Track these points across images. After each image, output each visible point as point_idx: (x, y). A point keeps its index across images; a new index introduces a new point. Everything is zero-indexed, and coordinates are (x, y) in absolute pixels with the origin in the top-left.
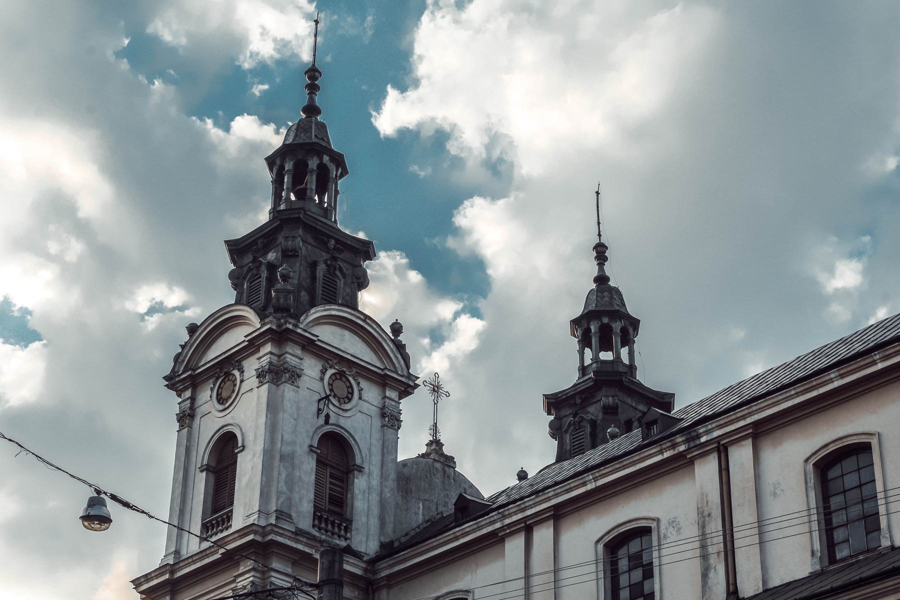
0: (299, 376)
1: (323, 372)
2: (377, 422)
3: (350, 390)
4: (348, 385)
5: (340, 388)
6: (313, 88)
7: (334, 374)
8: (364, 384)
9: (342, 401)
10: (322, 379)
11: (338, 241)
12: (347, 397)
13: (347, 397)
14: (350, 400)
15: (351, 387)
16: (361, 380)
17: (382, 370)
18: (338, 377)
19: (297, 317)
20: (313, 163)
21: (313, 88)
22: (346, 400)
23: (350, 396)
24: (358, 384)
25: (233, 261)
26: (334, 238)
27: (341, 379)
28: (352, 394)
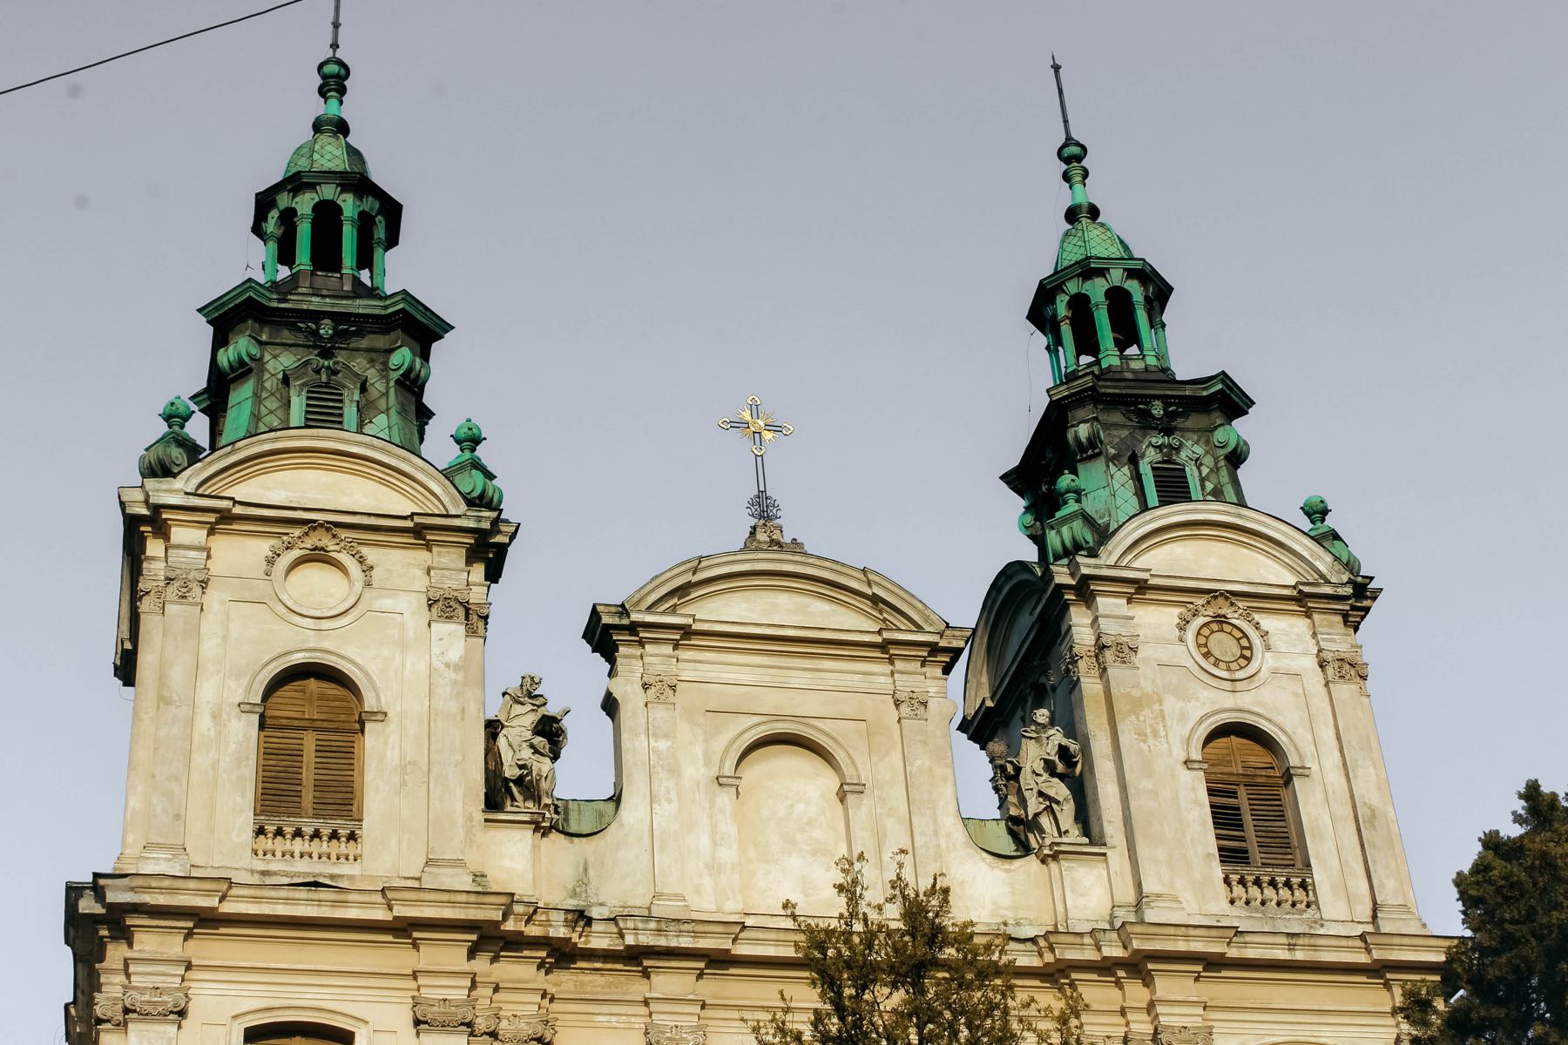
0: (1134, 650)
1: (1183, 625)
2: (1315, 678)
3: (1244, 642)
4: (1239, 635)
5: (1223, 645)
7: (1206, 625)
8: (1268, 622)
9: (1234, 666)
12: (1243, 656)
13: (1243, 656)
14: (1249, 660)
15: (1245, 636)
18: (1215, 627)
19: (1093, 554)
20: (1096, 290)
22: (1243, 662)
25: (1021, 494)
28: (1250, 648)
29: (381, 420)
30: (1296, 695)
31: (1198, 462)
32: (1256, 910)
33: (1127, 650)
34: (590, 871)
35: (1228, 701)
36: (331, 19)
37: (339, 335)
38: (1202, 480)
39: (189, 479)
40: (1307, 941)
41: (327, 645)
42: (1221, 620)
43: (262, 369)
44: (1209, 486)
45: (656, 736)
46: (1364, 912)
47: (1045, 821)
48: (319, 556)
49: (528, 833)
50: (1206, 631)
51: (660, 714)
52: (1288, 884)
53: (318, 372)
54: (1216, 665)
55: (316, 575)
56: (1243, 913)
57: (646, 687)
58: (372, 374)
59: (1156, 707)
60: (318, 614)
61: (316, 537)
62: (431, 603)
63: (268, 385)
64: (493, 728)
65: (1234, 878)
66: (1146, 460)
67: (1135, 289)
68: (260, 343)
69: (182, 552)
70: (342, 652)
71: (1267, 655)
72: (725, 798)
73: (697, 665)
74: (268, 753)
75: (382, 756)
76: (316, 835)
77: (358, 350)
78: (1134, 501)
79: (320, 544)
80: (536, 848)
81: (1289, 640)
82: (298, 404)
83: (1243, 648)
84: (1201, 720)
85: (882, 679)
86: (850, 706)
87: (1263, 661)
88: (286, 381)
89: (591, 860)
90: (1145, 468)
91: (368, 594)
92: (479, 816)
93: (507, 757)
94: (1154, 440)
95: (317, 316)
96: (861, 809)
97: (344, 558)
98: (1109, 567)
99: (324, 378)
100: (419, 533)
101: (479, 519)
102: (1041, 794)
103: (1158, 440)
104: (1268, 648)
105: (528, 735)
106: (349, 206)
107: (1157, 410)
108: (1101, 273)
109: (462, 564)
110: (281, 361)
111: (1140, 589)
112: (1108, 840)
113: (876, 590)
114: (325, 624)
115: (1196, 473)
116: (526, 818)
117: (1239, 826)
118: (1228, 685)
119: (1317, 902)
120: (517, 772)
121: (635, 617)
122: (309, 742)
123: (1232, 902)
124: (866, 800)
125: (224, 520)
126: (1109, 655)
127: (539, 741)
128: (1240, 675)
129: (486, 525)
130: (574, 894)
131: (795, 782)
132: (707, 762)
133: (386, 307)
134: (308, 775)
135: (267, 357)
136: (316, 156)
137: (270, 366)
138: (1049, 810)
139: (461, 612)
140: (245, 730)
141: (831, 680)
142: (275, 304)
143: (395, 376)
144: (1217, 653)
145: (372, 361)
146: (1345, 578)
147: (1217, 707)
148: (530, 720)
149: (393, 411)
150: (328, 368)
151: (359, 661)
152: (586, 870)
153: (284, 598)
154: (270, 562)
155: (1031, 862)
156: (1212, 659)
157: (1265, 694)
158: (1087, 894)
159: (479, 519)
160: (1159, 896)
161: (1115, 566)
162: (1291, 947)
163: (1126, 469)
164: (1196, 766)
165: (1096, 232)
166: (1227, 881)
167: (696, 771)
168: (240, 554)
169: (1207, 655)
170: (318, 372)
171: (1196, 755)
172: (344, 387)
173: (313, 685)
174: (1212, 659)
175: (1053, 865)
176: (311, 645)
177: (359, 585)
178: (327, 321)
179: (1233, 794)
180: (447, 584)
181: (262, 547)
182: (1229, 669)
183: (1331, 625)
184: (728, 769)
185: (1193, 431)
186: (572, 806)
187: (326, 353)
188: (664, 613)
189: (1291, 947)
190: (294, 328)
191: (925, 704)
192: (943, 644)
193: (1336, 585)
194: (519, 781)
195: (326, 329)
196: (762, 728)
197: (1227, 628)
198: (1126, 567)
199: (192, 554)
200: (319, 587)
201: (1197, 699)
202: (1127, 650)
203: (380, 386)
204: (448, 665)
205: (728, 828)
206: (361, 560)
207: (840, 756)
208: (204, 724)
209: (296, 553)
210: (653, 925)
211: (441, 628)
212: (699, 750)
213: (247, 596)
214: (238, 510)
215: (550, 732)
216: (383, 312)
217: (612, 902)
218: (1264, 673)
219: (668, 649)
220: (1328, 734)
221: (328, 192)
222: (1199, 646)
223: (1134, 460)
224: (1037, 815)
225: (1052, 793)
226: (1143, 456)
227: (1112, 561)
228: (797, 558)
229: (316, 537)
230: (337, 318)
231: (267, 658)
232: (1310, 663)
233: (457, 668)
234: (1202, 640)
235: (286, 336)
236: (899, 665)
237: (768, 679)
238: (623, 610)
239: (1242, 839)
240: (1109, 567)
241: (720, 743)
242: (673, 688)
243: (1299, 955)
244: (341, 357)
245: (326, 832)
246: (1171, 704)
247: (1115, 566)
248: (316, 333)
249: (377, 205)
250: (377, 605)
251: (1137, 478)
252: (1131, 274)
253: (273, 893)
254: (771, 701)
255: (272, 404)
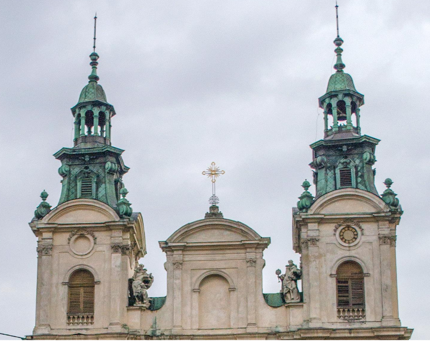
1: (335, 231)
2: (376, 244)
5: (349, 235)
6: (339, 51)
7: (343, 229)
8: (364, 226)
9: (351, 241)
10: (335, 235)
11: (348, 145)
12: (354, 238)
14: (356, 239)
15: (356, 231)
16: (361, 224)
17: (372, 214)
18: (346, 229)
21: (339, 51)
22: (354, 240)
23: (356, 237)
24: (360, 228)
26: (345, 145)
27: (349, 230)
28: (357, 235)
29: (103, 186)
30: (370, 249)
31: (356, 167)
32: (346, 320)
33: (314, 241)
34: (157, 320)
35: (347, 254)
36: (93, 37)
37: (90, 159)
38: (357, 173)
39: (45, 220)
40: (355, 331)
41: (85, 263)
42: (348, 227)
43: (70, 173)
44: (360, 174)
45: (176, 279)
46: (379, 318)
47: (288, 295)
48: (82, 236)
49: (139, 312)
50: (343, 231)
51: (178, 273)
52: (358, 310)
53: (84, 174)
54: (345, 242)
55: (82, 243)
56: (342, 321)
57: (174, 264)
58: (100, 171)
59: (323, 258)
60: (82, 254)
61: (81, 231)
62: (112, 247)
63: (72, 178)
64: (131, 281)
65: (341, 310)
66: (338, 168)
67: (348, 101)
68: (70, 165)
69: (46, 240)
70: (88, 265)
71: (363, 237)
72: (196, 296)
73: (190, 257)
74: (71, 294)
75: (100, 293)
76: (83, 317)
77: (97, 163)
78: (333, 182)
79: (82, 233)
80: (141, 315)
81: (370, 232)
82: (79, 184)
83: (355, 235)
84: (337, 261)
85: (243, 255)
86: (233, 264)
87: (361, 239)
88: (76, 177)
89: (157, 317)
90: (338, 171)
91: (96, 246)
92: (126, 309)
93: (134, 290)
94: (341, 161)
95: (83, 155)
96: (234, 295)
97: (89, 236)
98: (311, 215)
99: (86, 175)
100: (108, 227)
101: (124, 222)
102: (287, 287)
103: (342, 161)
104: (362, 234)
105: (140, 282)
106: (96, 112)
107: (345, 148)
108: (336, 96)
109: (121, 235)
110: (76, 170)
111: (321, 221)
112: (304, 301)
113: (241, 228)
114: (84, 257)
115: (354, 171)
116: (138, 308)
117: (347, 291)
118: (348, 248)
119: (365, 316)
120: (137, 294)
121: (170, 244)
122: (82, 290)
123: (339, 317)
124: (236, 293)
125: (56, 230)
126: (309, 243)
127: (143, 284)
128: (351, 245)
129: (126, 223)
130: (152, 327)
131: (215, 288)
132: (191, 286)
133: (103, 150)
134: (82, 299)
135: (71, 169)
136: (87, 94)
137: (72, 173)
138: (289, 292)
139: (120, 250)
140: (63, 291)
141: (228, 256)
142: (72, 153)
143: (107, 171)
144: (346, 238)
145: (100, 166)
146: (388, 210)
147: (343, 256)
148: (141, 277)
149: (106, 182)
150: (87, 172)
151: (93, 267)
152: (155, 320)
153: (73, 250)
154: (69, 240)
155: (283, 309)
156: (344, 240)
157: (359, 250)
158: (295, 318)
159: (124, 222)
160: (315, 318)
161: (314, 214)
162: (350, 333)
163: (332, 171)
164: (334, 276)
165: (338, 77)
166: (339, 311)
167: (188, 288)
168: (61, 239)
169: (342, 239)
170: (84, 174)
171: (334, 272)
172: (92, 177)
173: (82, 274)
174: (344, 240)
175: (288, 309)
176: (80, 263)
177: (93, 244)
178: (87, 156)
179: (347, 282)
180: (117, 241)
181: (67, 235)
182: (349, 243)
183: (384, 225)
184: (197, 287)
185: (357, 154)
186: (156, 299)
187: (87, 168)
188: (178, 242)
189: (350, 333)
190: (78, 158)
191: (255, 262)
192: (261, 242)
193: (387, 212)
194: (137, 296)
195: (87, 159)
196: (207, 273)
197: (350, 229)
198: (318, 214)
199: (49, 240)
200: (83, 246)
201: (337, 254)
202: (314, 241)
203: (103, 175)
204: (116, 266)
205: (196, 304)
206: (93, 236)
207: (229, 280)
208: (54, 290)
209: (76, 236)
210: (168, 337)
211: (114, 255)
212: (189, 282)
213: (64, 250)
214: (60, 226)
215: (147, 282)
216: (102, 151)
217: (162, 329)
218: (360, 243)
219: (180, 252)
220: (377, 262)
221: (89, 108)
222: (340, 236)
223: (335, 168)
224: (286, 293)
225: (290, 287)
226: (337, 166)
227: (312, 213)
228: (218, 220)
229: (81, 231)
230: (90, 154)
231: (69, 268)
232: (375, 238)
233: (119, 267)
234: (342, 234)
235: (77, 162)
236: (248, 250)
237: (210, 258)
238: (166, 243)
239: (348, 296)
240: (311, 215)
241: (194, 279)
242: (181, 264)
243: (352, 335)
244: (91, 168)
245: (85, 316)
246: (329, 256)
247: (314, 214)
248: (84, 160)
249: (105, 108)
250: (98, 250)
251: (335, 174)
252: (346, 95)
253: (69, 337)
254: (210, 265)
255: (73, 185)
